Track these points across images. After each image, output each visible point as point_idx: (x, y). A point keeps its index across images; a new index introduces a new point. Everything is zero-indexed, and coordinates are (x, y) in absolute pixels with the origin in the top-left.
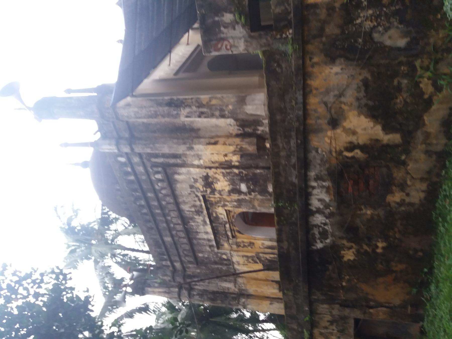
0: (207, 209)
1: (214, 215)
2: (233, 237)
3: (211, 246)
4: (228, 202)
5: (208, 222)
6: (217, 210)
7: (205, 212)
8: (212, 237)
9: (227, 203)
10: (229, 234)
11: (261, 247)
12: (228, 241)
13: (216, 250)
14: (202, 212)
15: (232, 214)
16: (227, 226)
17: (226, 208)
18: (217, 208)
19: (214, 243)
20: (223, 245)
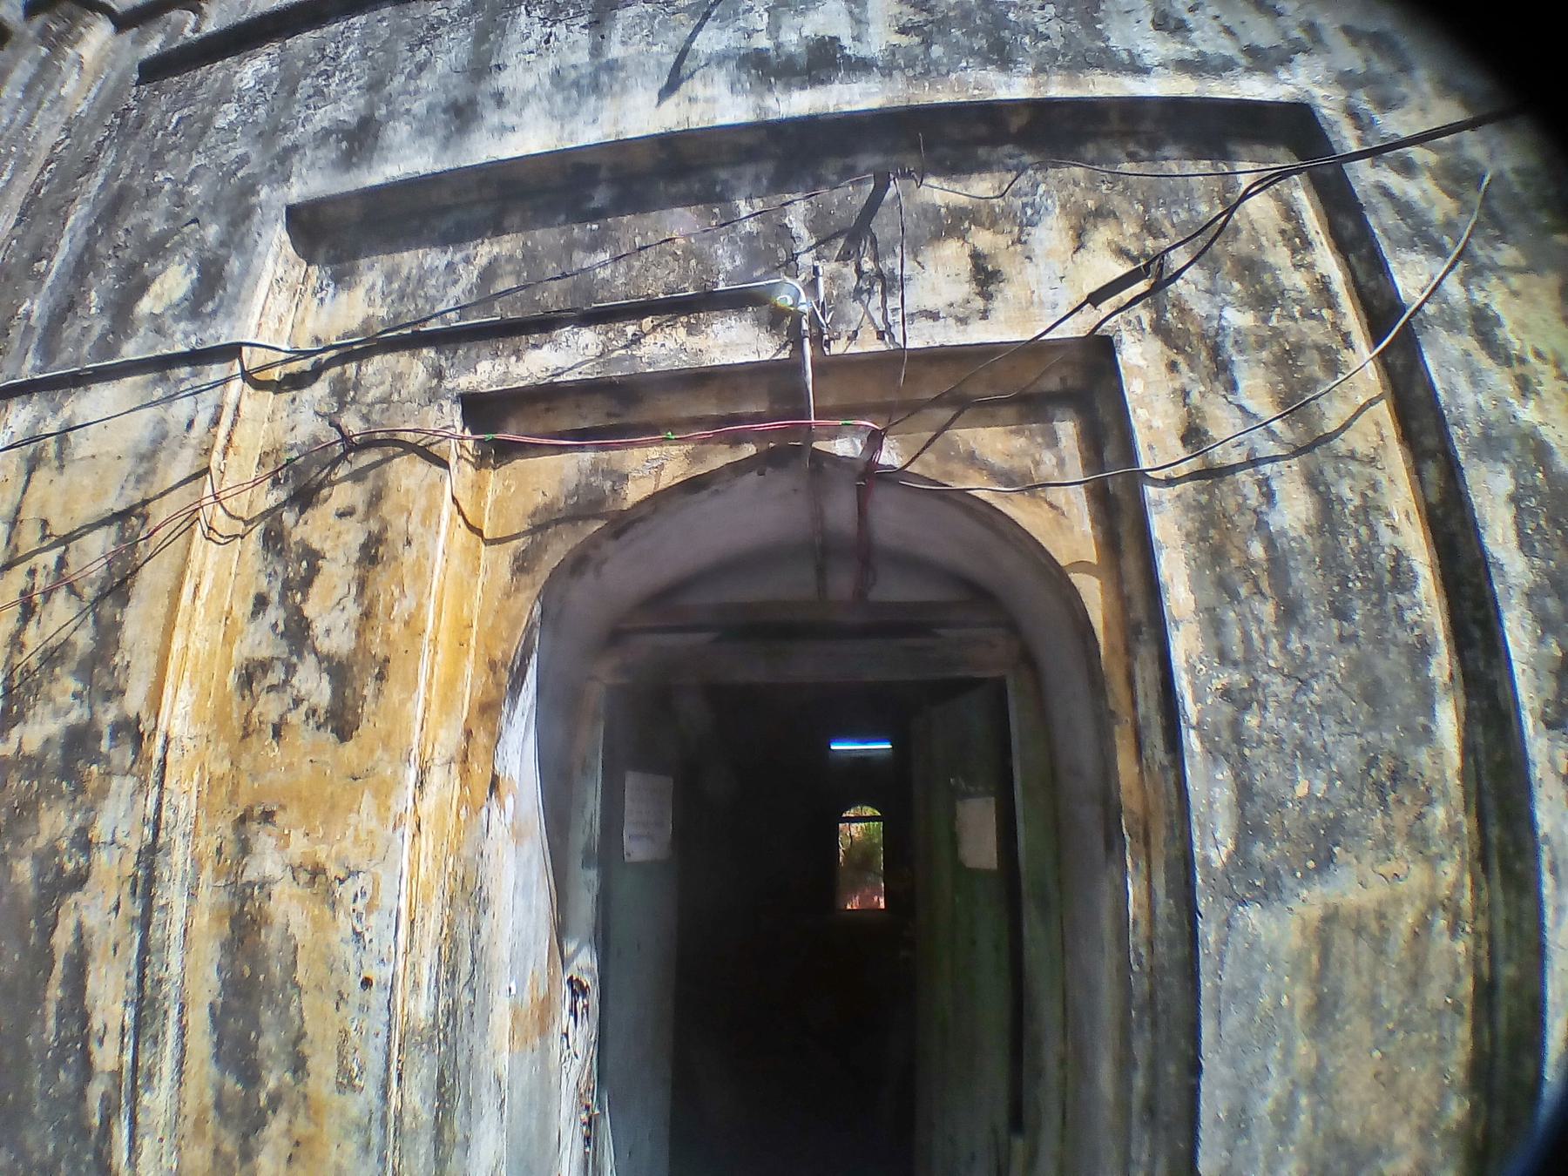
0: (1056, 131)
1: (939, 192)
2: (481, 410)
3: (360, 139)
4: (1295, 404)
5: (799, 103)
6: (1051, 234)
7: (1014, 87)
8: (526, 134)
9: (1255, 387)
10: (540, 362)
11: (268, 861)
12: (413, 342)
13: (310, 182)
14: (1001, 56)
15: (994, 442)
16: (735, 342)
17: (1138, 357)
18: (1102, 235)
19: (407, 158)
20: (342, 278)
